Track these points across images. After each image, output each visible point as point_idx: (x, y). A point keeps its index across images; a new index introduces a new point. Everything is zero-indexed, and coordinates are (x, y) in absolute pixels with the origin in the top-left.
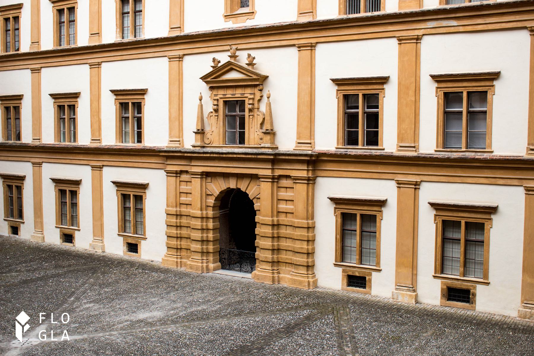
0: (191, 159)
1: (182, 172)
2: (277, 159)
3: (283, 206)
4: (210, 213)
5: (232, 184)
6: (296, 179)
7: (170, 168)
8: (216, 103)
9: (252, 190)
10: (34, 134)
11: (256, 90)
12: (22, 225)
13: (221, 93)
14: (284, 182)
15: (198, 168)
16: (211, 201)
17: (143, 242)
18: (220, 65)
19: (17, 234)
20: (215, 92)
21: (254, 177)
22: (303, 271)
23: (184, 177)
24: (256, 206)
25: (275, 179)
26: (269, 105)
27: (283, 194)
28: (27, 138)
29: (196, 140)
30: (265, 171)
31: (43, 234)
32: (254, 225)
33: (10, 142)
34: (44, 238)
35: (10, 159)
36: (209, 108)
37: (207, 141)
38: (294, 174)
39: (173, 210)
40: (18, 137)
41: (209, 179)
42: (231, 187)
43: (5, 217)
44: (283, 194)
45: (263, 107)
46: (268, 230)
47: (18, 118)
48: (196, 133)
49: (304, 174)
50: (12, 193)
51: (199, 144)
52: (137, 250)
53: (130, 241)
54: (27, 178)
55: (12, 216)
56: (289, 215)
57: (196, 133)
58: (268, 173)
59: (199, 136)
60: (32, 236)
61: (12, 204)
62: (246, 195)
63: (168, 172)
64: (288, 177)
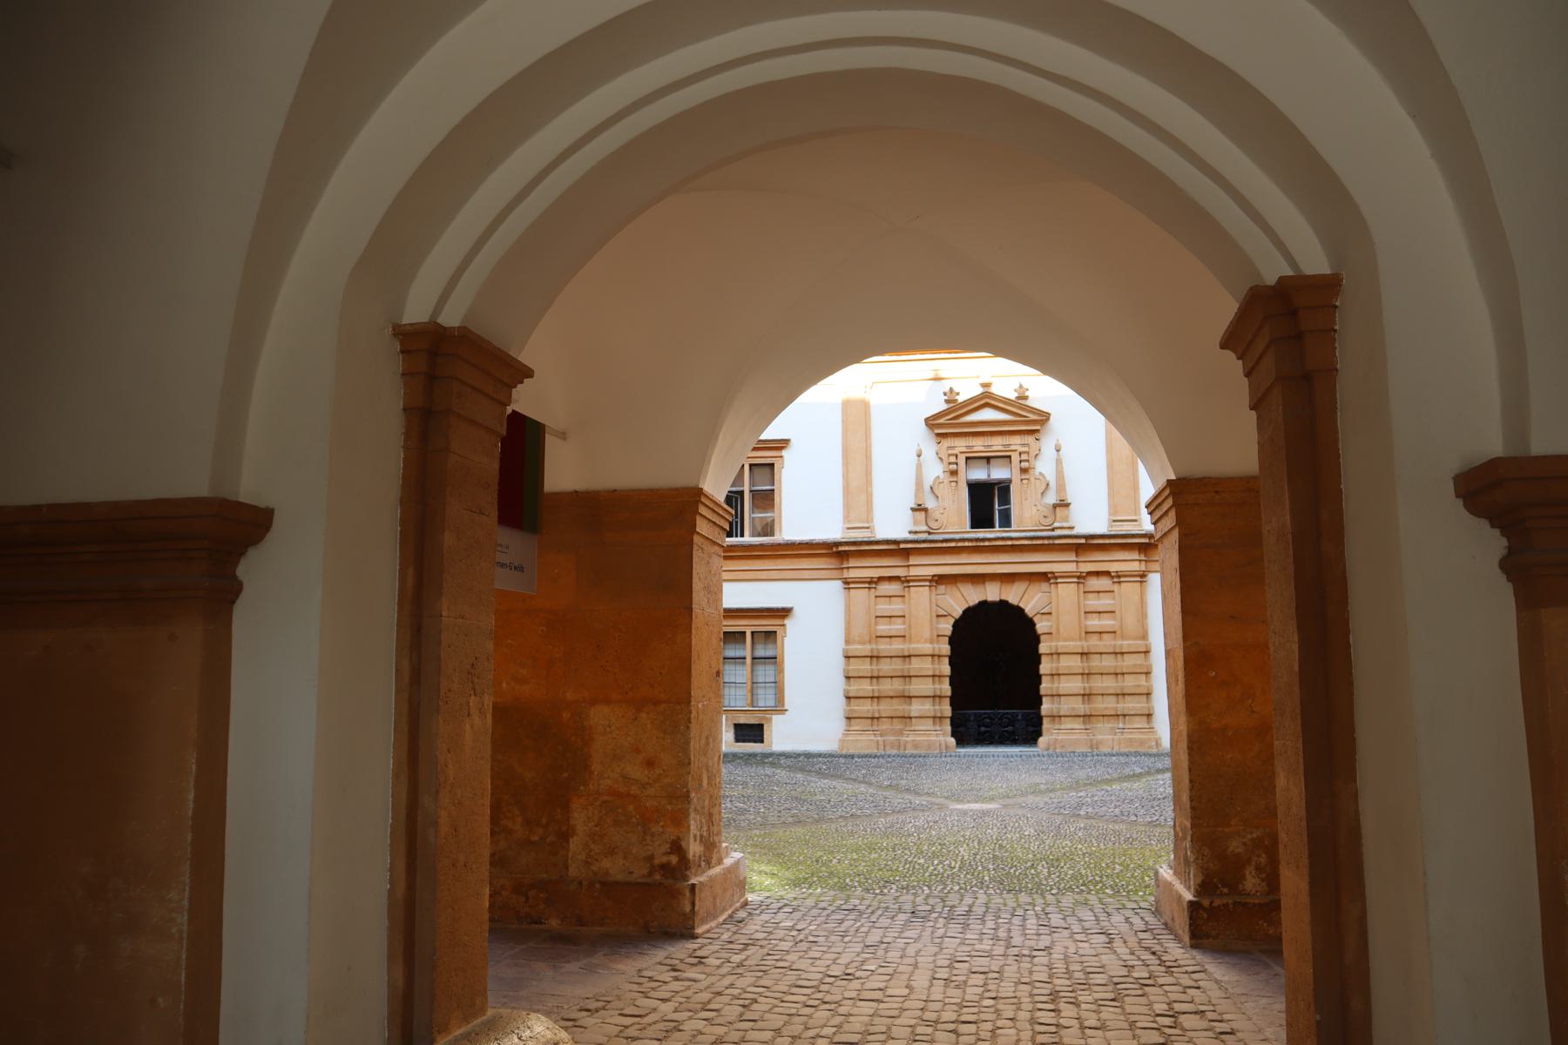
0: (906, 553)
1: (881, 579)
2: (1088, 545)
3: (1094, 623)
4: (946, 649)
5: (992, 593)
6: (1117, 577)
7: (853, 574)
8: (953, 459)
9: (1030, 600)
11: (1030, 439)
13: (961, 445)
14: (1094, 583)
15: (925, 567)
16: (947, 627)
17: (776, 718)
18: (961, 399)
20: (947, 442)
21: (1044, 577)
22: (1140, 723)
23: (885, 588)
24: (1041, 626)
25: (1081, 578)
26: (1059, 462)
27: (1094, 602)
29: (915, 523)
30: (1062, 564)
32: (1037, 659)
36: (934, 470)
37: (934, 525)
38: (1113, 568)
39: (859, 649)
41: (942, 588)
42: (990, 598)
44: (1094, 602)
45: (1044, 466)
46: (1075, 663)
48: (913, 510)
49: (1135, 566)
51: (925, 528)
52: (762, 735)
53: (743, 720)
56: (1105, 636)
57: (913, 510)
58: (1071, 567)
59: (921, 515)
62: (1018, 612)
63: (846, 582)
64: (1107, 573)
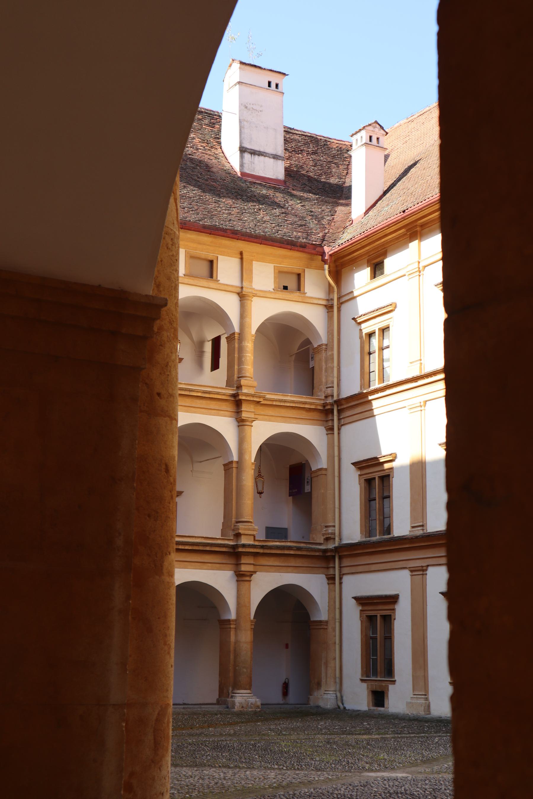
10: (413, 517)
12: (391, 687)
19: (383, 705)
28: (401, 527)
31: (427, 699)
33: (374, 539)
34: (429, 706)
35: (373, 567)
40: (389, 530)
43: (362, 675)
47: (387, 497)
50: (375, 632)
54: (401, 599)
55: (375, 674)
60: (408, 703)
61: (375, 653)
